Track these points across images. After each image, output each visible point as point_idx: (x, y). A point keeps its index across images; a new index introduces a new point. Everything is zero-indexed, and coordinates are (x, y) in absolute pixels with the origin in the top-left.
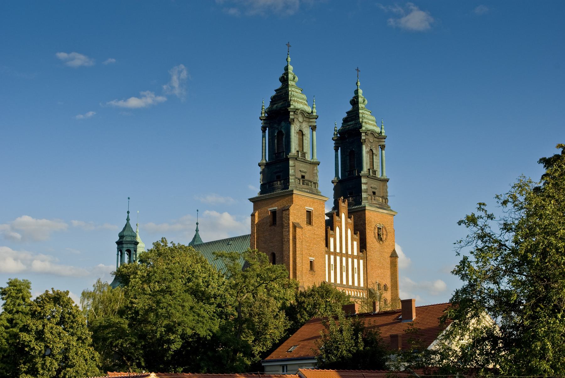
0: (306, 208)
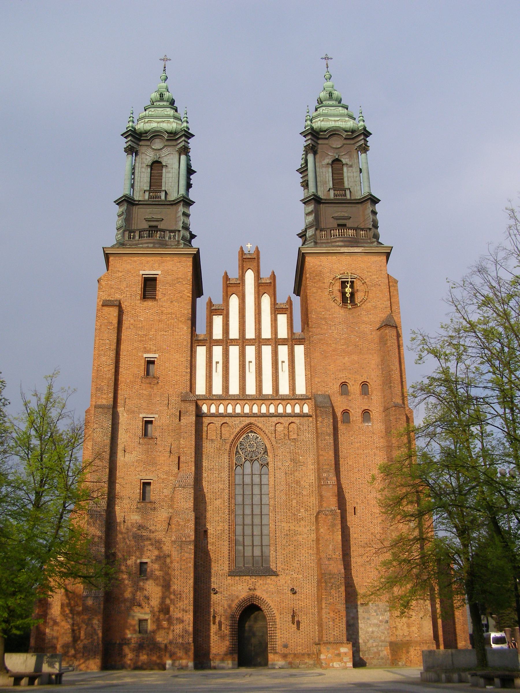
0: (142, 272)
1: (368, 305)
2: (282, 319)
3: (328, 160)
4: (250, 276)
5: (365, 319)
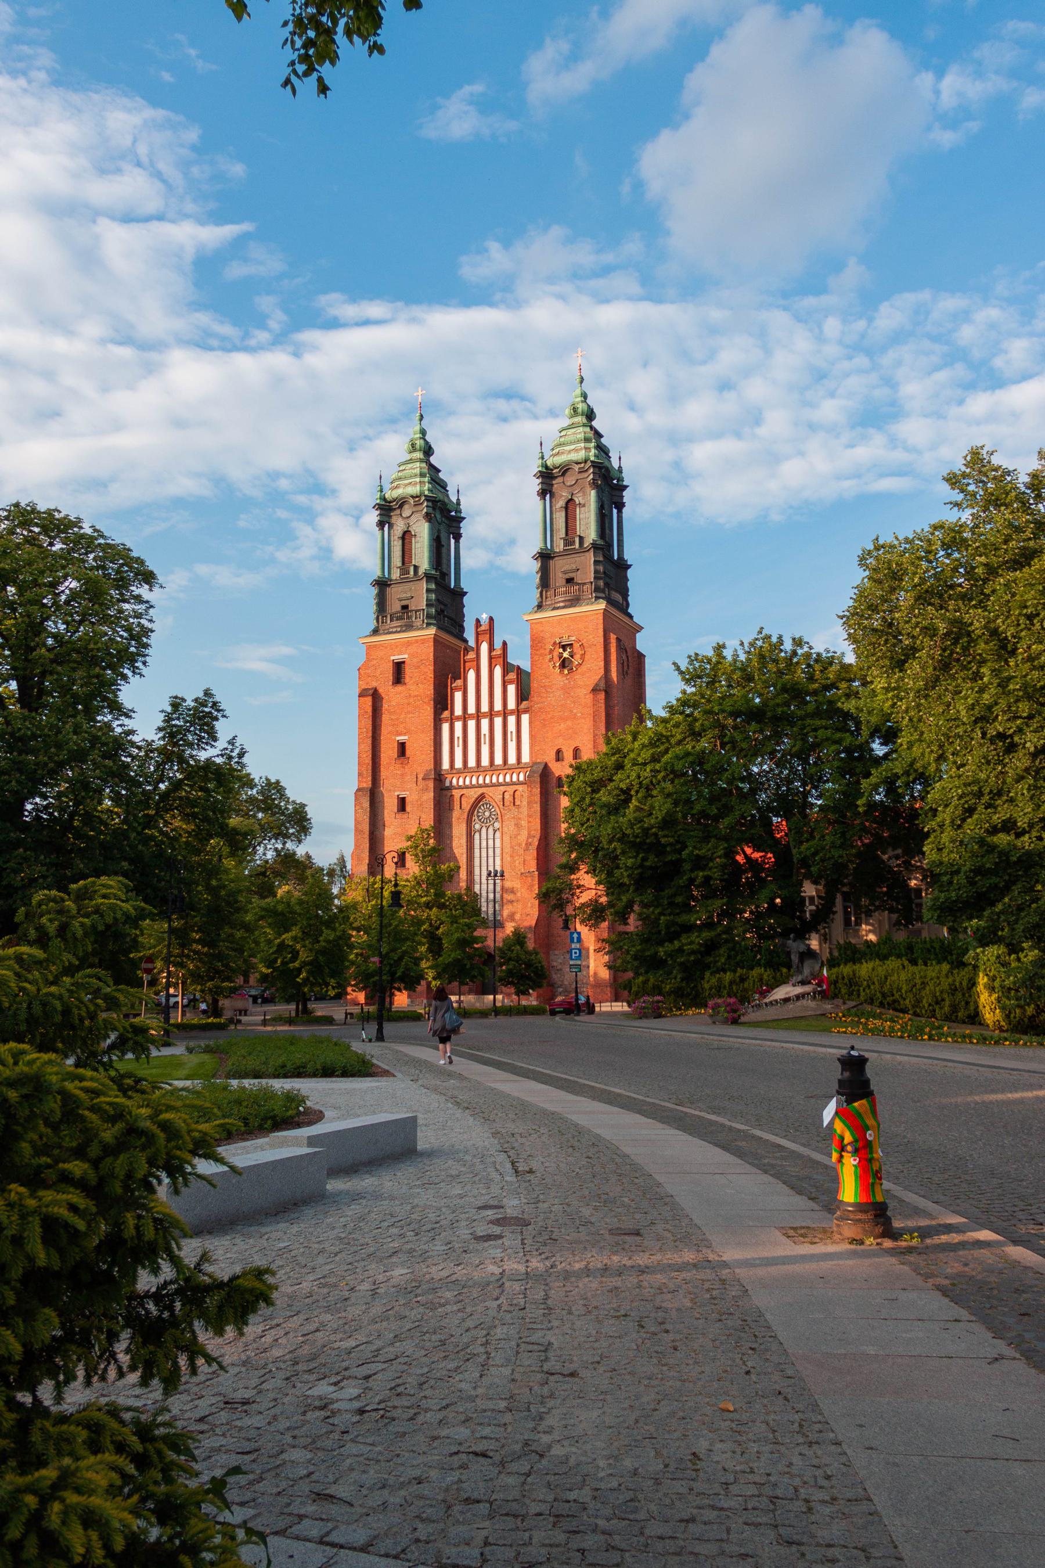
1: (584, 668)
2: (512, 689)
3: (561, 503)
4: (484, 647)
5: (580, 683)
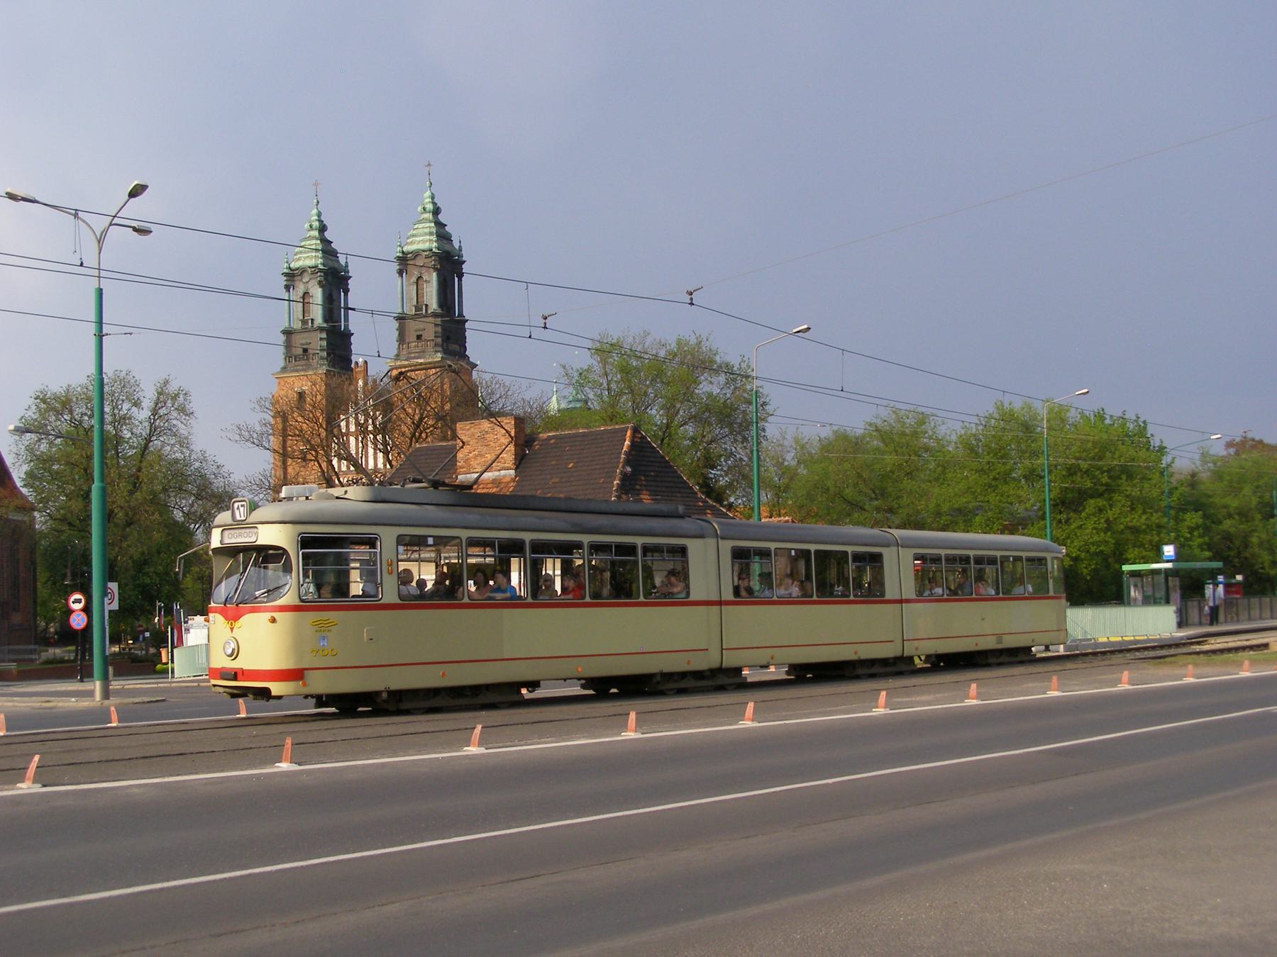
3: (414, 279)
